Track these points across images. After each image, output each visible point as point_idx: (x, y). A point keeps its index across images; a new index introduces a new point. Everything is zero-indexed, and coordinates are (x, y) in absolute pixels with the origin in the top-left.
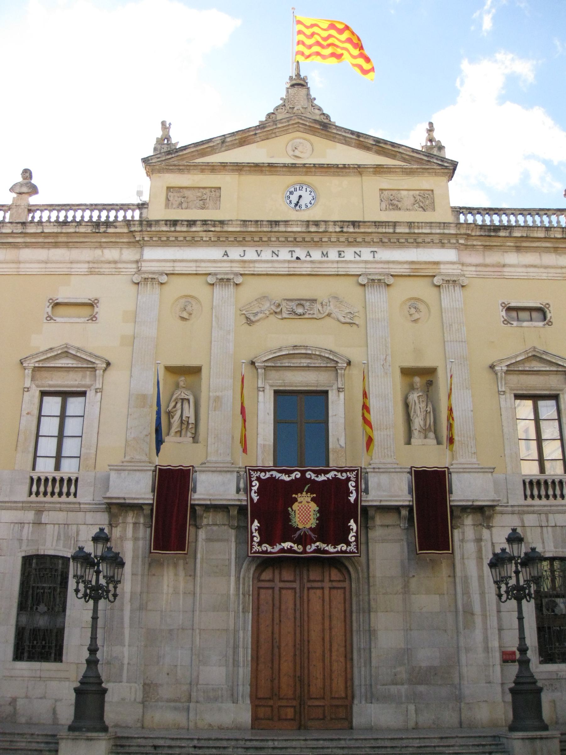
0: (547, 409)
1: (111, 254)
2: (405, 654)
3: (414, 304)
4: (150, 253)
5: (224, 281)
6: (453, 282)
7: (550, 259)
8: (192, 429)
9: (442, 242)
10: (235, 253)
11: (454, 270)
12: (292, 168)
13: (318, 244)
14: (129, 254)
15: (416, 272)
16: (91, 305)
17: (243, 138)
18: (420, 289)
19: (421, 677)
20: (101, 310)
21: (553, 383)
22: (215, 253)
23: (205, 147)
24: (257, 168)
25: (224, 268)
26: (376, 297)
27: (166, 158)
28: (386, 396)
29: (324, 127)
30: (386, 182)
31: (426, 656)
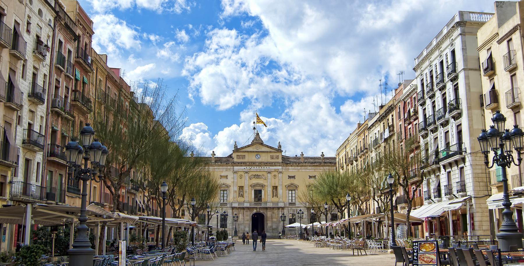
0: (293, 192)
1: (229, 167)
2: (272, 226)
3: (275, 176)
4: (235, 168)
5: (247, 173)
6: (281, 172)
7: (296, 168)
8: (242, 196)
9: (279, 166)
10: (248, 167)
11: (281, 170)
12: (257, 152)
13: (260, 166)
14: (232, 168)
15: (276, 170)
16: (227, 176)
17: (249, 146)
18: (276, 173)
19: (273, 229)
20: (228, 177)
21: (295, 188)
22: (245, 167)
23: (242, 148)
24: (251, 152)
25: (246, 170)
26: (269, 175)
27: (237, 150)
28: (270, 190)
29: (262, 144)
30: (272, 154)
31: (274, 227)
